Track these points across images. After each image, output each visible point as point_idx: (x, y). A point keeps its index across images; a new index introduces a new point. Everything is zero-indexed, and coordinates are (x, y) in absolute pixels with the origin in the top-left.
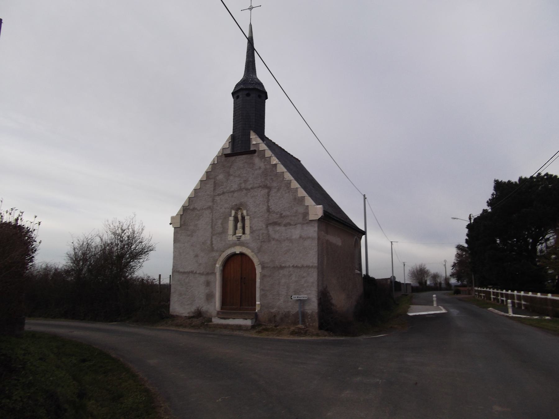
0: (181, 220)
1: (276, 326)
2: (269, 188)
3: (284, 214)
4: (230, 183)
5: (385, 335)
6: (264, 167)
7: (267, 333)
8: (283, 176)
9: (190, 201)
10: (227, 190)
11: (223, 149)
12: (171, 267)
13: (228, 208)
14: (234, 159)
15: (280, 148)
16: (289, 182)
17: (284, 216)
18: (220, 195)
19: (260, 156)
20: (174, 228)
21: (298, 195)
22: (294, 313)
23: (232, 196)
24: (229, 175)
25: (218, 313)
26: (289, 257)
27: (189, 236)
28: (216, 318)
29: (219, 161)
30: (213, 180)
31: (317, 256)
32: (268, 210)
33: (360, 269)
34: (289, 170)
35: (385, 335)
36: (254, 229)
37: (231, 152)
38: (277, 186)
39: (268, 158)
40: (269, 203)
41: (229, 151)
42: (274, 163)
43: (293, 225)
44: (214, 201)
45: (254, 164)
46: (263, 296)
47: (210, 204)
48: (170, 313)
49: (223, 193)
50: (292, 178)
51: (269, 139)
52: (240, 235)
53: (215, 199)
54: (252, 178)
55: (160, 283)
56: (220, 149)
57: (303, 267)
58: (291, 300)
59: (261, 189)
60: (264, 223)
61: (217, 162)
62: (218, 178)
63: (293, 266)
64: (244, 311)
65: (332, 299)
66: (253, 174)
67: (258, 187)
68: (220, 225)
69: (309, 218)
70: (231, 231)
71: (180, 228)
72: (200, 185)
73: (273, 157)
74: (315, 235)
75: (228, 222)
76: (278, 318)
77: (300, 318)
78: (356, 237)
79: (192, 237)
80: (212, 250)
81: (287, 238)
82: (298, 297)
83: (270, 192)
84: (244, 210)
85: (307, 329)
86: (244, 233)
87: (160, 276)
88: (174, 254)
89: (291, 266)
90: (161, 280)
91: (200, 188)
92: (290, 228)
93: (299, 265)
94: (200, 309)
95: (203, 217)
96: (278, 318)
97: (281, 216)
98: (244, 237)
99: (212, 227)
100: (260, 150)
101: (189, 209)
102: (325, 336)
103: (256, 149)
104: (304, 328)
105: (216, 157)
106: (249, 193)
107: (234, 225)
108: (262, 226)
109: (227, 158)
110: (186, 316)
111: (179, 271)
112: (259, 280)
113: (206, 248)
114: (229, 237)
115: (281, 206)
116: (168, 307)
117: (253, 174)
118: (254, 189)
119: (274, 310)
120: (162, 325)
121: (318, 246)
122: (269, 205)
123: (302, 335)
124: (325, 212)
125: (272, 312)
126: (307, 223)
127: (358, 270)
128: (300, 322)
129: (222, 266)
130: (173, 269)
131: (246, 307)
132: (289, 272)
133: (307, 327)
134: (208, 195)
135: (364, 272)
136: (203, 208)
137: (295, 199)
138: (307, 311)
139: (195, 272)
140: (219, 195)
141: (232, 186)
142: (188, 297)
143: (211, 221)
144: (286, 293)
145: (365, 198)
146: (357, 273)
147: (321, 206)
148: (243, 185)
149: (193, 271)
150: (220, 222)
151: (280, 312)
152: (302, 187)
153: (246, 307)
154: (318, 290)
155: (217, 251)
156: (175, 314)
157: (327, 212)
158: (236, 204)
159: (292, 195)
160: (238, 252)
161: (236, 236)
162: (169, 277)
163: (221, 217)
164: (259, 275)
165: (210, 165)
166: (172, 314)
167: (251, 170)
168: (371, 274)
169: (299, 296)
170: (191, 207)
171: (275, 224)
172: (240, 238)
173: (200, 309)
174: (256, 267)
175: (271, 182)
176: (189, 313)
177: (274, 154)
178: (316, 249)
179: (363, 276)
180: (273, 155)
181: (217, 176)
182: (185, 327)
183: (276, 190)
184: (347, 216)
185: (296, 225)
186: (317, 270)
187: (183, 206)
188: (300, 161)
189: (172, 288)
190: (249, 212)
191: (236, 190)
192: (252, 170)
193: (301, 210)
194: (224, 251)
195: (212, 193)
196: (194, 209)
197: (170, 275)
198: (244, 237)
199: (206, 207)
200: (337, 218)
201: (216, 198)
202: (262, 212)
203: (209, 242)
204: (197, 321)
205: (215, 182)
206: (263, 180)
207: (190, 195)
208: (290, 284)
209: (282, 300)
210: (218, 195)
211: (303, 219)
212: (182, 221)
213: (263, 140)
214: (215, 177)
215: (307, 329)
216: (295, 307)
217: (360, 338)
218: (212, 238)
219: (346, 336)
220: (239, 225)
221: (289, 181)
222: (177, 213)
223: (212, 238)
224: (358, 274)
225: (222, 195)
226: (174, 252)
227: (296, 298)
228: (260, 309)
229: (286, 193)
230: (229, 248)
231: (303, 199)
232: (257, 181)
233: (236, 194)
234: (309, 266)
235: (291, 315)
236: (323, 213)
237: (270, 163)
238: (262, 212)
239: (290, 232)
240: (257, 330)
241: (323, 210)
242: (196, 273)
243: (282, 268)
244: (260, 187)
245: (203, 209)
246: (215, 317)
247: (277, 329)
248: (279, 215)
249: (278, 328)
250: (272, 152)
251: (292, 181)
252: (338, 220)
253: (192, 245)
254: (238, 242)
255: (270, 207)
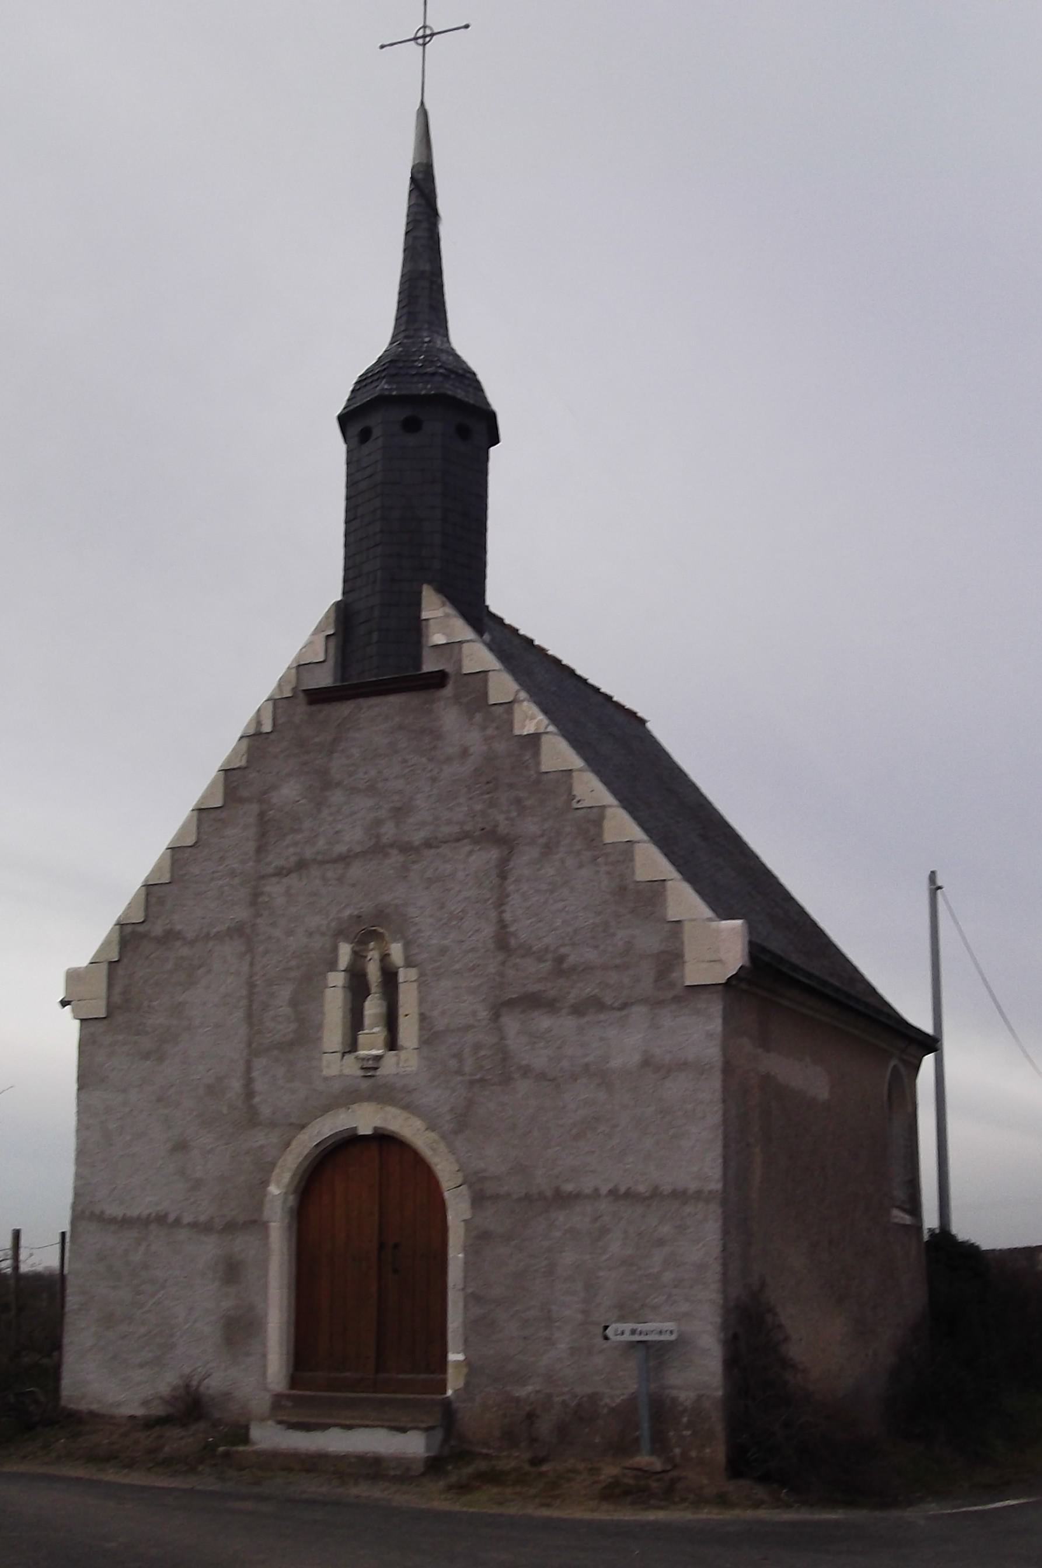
0: (110, 986)
1: (536, 1462)
2: (507, 843)
3: (572, 960)
4: (331, 819)
5: (1022, 1501)
6: (485, 748)
7: (495, 1490)
8: (570, 789)
9: (153, 900)
10: (318, 853)
11: (301, 667)
12: (69, 1198)
13: (323, 934)
14: (346, 713)
15: (556, 662)
16: (597, 817)
17: (573, 969)
18: (284, 872)
19: (465, 700)
20: (82, 1020)
21: (633, 872)
22: (618, 1401)
23: (340, 880)
24: (326, 783)
25: (278, 1402)
26: (593, 1152)
27: (146, 1056)
28: (270, 1422)
29: (280, 721)
30: (254, 808)
31: (718, 1149)
32: (503, 941)
33: (914, 1206)
34: (596, 763)
35: (1022, 1501)
36: (441, 1024)
37: (335, 680)
38: (542, 836)
39: (501, 709)
40: (507, 908)
41: (324, 679)
42: (529, 728)
43: (612, 1008)
44: (260, 899)
45: (436, 735)
46: (476, 1327)
47: (241, 914)
48: (63, 1402)
49: (302, 865)
50: (607, 798)
51: (507, 621)
52: (375, 1052)
53: (262, 894)
54: (429, 796)
55: (16, 1267)
56: (284, 671)
57: (656, 1194)
58: (606, 1345)
59: (468, 848)
60: (484, 1000)
61: (274, 725)
62: (275, 798)
63: (613, 1193)
64: (394, 1392)
65: (787, 1339)
66: (434, 780)
67: (458, 840)
68: (286, 1010)
69: (682, 977)
70: (333, 1035)
71: (105, 1022)
72: (194, 829)
73: (525, 703)
74: (713, 1053)
75: (322, 992)
76: (545, 1427)
77: (645, 1425)
78: (893, 1062)
79: (161, 1059)
80: (252, 1119)
81: (587, 1065)
82: (633, 1332)
83: (508, 860)
84: (395, 941)
85: (675, 1474)
86: (392, 1044)
87: (17, 1235)
88: (78, 1138)
89: (604, 1191)
90: (23, 1254)
91: (196, 842)
92: (599, 1022)
93: (641, 1188)
94: (194, 1383)
95: (209, 971)
96: (545, 1427)
97: (561, 969)
98: (394, 1060)
99: (249, 1016)
100: (465, 671)
101: (144, 936)
102: (757, 1505)
103: (449, 668)
104: (664, 1472)
105: (271, 703)
106: (414, 862)
107: (349, 1006)
108: (474, 1013)
109: (314, 708)
110: (132, 1417)
111: (102, 1212)
112: (461, 1255)
113: (225, 1110)
114: (324, 1063)
115: (558, 922)
116: (54, 1374)
117: (434, 780)
118: (437, 847)
119: (530, 1388)
120: (24, 1457)
121: (724, 1101)
122: (507, 917)
123: (652, 1502)
124: (756, 950)
125: (518, 1400)
126: (677, 999)
127: (904, 1210)
128: (646, 1444)
129: (295, 1192)
130: (74, 1206)
131: (401, 1376)
132: (596, 1219)
133: (675, 1466)
134: (233, 874)
135: (930, 1220)
136: (208, 934)
137: (621, 891)
138: (674, 1393)
139: (171, 1218)
140: (281, 873)
141: (337, 832)
142: (143, 1330)
143: (244, 992)
144: (584, 1312)
145: (935, 888)
146: (902, 1222)
147: (739, 922)
148: (389, 830)
149: (166, 1215)
150: (285, 992)
151: (557, 1399)
152: (651, 837)
153: (401, 1376)
154: (726, 1299)
155: (273, 1125)
156: (83, 1406)
157: (764, 950)
158: (356, 913)
159: (608, 873)
160: (365, 1130)
161: (357, 1058)
162: (58, 1239)
163: (293, 974)
164: (461, 1231)
165: (242, 737)
166: (72, 1406)
167: (424, 760)
168: (963, 1229)
169: (640, 1327)
170: (158, 929)
171: (532, 1002)
172: (376, 1069)
173: (194, 1383)
174: (446, 1195)
175: (514, 814)
176: (145, 1403)
177: (528, 691)
178: (714, 1116)
179: (926, 1237)
180: (523, 695)
181: (274, 787)
182: (131, 1465)
183: (534, 852)
184: (855, 969)
185: (624, 1006)
186: (719, 1211)
187: (121, 925)
188: (642, 722)
189: (69, 1290)
190: (416, 951)
191: (358, 849)
192: (430, 760)
193: (649, 941)
194: (303, 1127)
195: (251, 864)
196: (170, 937)
197: (63, 1234)
198: (394, 1060)
199: (224, 927)
200: (810, 976)
201: (268, 889)
202: (473, 950)
203: (236, 1085)
204: (182, 1438)
205: (262, 815)
206: (479, 807)
207: (153, 871)
208: (601, 1274)
209: (562, 1346)
210: (274, 875)
211: (656, 981)
212: (117, 990)
213: (479, 629)
214: (265, 793)
215: (675, 1474)
216: (621, 1373)
217: (911, 1514)
218: (249, 1069)
219: (850, 1504)
220: (373, 1007)
221: (595, 810)
222: (92, 959)
223: (249, 1069)
224: (905, 1226)
225: (294, 875)
226: (82, 1127)
227: (627, 1337)
228: (467, 1384)
229: (581, 866)
230: (326, 1109)
231: (657, 888)
232: (451, 809)
233: (356, 871)
234: (684, 1192)
235: (605, 1411)
236: (746, 958)
237: (512, 730)
238: (473, 950)
239: (602, 1039)
240: (453, 1479)
241: (747, 939)
242: (177, 1222)
243: (562, 1199)
244: (463, 836)
245: (207, 937)
246: (263, 1420)
247: (542, 1474)
248: (549, 963)
249: (545, 1468)
250: (517, 679)
251: (609, 812)
252: (813, 983)
253: (159, 1100)
254: (365, 1085)
255: (512, 929)
